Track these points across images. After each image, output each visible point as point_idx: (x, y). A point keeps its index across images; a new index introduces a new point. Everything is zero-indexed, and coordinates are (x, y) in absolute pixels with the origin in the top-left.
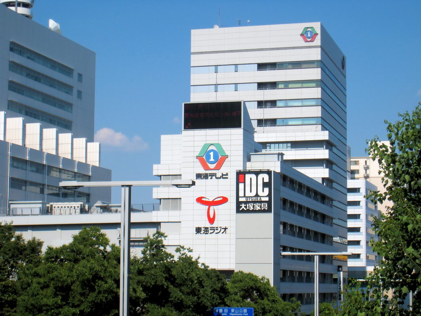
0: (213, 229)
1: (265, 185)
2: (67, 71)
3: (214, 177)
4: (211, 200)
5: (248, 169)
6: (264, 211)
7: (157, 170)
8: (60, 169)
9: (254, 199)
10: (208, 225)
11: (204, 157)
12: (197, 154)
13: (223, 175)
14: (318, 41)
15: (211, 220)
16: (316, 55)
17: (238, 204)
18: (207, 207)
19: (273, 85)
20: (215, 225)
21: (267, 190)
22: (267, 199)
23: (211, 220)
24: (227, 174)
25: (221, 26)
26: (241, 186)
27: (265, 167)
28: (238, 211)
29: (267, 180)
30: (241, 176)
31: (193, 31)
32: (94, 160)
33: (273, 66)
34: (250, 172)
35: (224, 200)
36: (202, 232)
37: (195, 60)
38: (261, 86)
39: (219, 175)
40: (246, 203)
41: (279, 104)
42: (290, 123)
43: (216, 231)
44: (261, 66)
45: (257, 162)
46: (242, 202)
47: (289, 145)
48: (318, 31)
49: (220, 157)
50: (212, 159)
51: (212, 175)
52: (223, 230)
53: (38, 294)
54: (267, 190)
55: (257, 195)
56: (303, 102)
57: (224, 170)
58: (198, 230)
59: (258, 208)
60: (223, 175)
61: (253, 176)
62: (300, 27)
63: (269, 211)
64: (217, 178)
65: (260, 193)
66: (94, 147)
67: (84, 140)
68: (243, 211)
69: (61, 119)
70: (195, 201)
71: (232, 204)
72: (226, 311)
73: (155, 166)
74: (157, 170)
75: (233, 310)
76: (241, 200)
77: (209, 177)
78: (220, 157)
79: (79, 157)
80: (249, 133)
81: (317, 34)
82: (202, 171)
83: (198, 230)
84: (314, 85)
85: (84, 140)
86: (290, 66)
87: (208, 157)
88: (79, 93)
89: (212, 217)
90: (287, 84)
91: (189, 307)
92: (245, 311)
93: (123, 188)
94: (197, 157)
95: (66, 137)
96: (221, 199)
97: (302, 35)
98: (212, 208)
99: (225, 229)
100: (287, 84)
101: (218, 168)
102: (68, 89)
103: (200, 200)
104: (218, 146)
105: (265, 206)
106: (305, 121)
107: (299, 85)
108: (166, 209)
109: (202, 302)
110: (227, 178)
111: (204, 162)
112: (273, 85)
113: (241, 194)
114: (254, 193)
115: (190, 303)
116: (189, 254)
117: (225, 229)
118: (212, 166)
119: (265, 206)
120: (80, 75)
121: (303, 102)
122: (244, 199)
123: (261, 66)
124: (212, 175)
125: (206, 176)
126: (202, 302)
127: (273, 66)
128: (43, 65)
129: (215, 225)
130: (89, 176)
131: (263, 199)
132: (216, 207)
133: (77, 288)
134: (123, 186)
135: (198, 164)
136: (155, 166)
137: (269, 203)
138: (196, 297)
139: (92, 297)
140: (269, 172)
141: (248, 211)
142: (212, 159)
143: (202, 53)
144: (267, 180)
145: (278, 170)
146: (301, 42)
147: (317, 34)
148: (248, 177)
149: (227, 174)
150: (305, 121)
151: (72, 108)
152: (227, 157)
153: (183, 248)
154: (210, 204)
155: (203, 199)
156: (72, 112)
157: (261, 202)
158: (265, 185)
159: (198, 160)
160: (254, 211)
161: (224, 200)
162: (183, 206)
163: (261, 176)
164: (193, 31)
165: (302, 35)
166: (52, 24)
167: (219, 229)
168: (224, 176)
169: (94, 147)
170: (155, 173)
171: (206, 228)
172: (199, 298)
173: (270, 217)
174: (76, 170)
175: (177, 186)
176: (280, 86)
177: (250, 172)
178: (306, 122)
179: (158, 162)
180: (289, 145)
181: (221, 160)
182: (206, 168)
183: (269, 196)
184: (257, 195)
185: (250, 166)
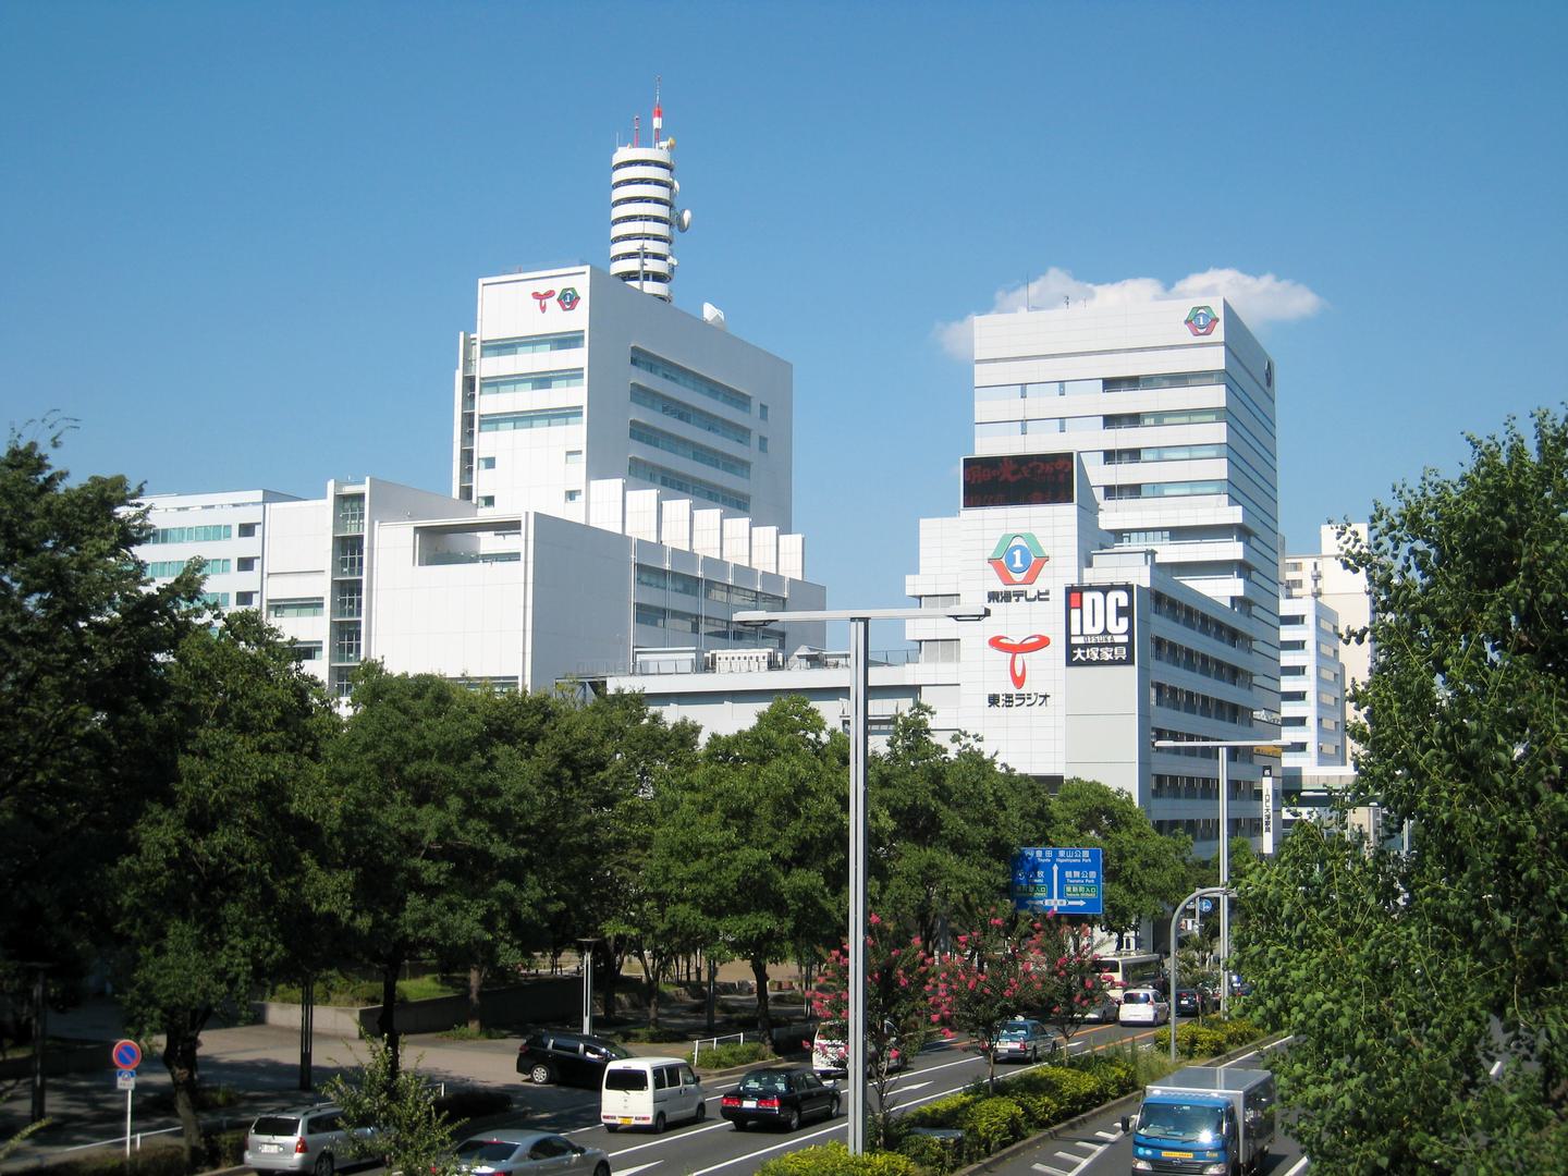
0: (1021, 697)
1: (1121, 612)
2: (740, 400)
4: (1017, 642)
5: (1087, 582)
6: (1120, 662)
7: (914, 585)
8: (728, 586)
9: (1101, 639)
10: (1013, 690)
11: (1003, 560)
12: (990, 554)
13: (1039, 594)
14: (1219, 333)
15: (1019, 681)
16: (1216, 359)
18: (1010, 655)
19: (1134, 419)
20: (1024, 690)
21: (1124, 622)
22: (1125, 639)
23: (1019, 681)
24: (1047, 593)
26: (1075, 614)
27: (1121, 580)
28: (1070, 662)
29: (1124, 602)
30: (1074, 594)
32: (792, 568)
33: (1133, 382)
34: (1091, 588)
35: (1043, 642)
36: (1001, 703)
38: (1111, 421)
39: (1031, 595)
40: (1085, 646)
41: (1145, 455)
42: (1167, 492)
43: (1028, 702)
44: (1110, 384)
45: (1105, 569)
46: (1076, 646)
47: (1167, 534)
48: (1220, 314)
49: (1033, 559)
50: (1018, 564)
51: (1019, 595)
52: (1040, 700)
53: (693, 823)
54: (1124, 622)
55: (1105, 632)
56: (1192, 450)
57: (1041, 584)
59: (1108, 657)
60: (1039, 594)
61: (1099, 596)
63: (1129, 661)
64: (1028, 600)
65: (1112, 628)
66: (792, 543)
67: (774, 529)
68: (1079, 663)
69: (728, 491)
70: (987, 645)
72: (1049, 853)
73: (909, 579)
74: (914, 585)
75: (1062, 853)
76: (1074, 641)
77: (1014, 599)
78: (1033, 559)
79: (764, 562)
80: (1088, 511)
81: (1217, 320)
82: (1000, 587)
83: (993, 700)
84: (1213, 418)
85: (774, 529)
86: (1166, 383)
88: (763, 440)
89: (1019, 673)
90: (1160, 417)
91: (979, 847)
92: (1086, 853)
95: (739, 525)
96: (1036, 640)
97: (1187, 322)
99: (1046, 697)
100: (1160, 417)
101: (1030, 580)
102: (741, 433)
103: (996, 642)
104: (1030, 538)
105: (1122, 653)
106: (1195, 487)
107: (1184, 419)
108: (930, 659)
109: (1002, 837)
110: (1047, 600)
112: (1134, 419)
113: (1075, 629)
114: (1099, 628)
115: (979, 839)
116: (976, 746)
117: (1046, 697)
118: (1018, 577)
119: (1122, 653)
120: (764, 408)
121: (1192, 450)
122: (1080, 640)
123: (1110, 384)
124: (1019, 595)
125: (1007, 597)
126: (1002, 837)
127: (1133, 382)
128: (695, 390)
130: (784, 599)
131: (1118, 639)
132: (1026, 656)
133: (764, 811)
134: (853, 619)
135: (991, 571)
136: (909, 579)
137: (1129, 646)
138: (991, 829)
139: (794, 828)
140: (1128, 588)
141: (1089, 663)
142: (1018, 564)
143: (995, 360)
144: (1124, 602)
145: (1146, 583)
147: (1217, 320)
148: (1087, 597)
149: (1047, 593)
150: (1195, 487)
151: (749, 471)
152: (1047, 559)
153: (965, 734)
154: (1014, 650)
155: (1002, 641)
156: (749, 478)
157: (1113, 645)
158: (1121, 612)
160: (1100, 663)
161: (1043, 642)
163: (1112, 596)
165: (1187, 322)
166: (710, 312)
167: (1034, 697)
168: (1042, 597)
169: (792, 543)
170: (909, 591)
171: (1009, 696)
172: (996, 829)
173: (1132, 672)
174: (759, 588)
175: (955, 617)
176: (1147, 421)
177: (1091, 588)
178: (1199, 490)
179: (916, 571)
180: (1167, 534)
181: (1036, 564)
182: (1008, 581)
183: (1130, 632)
184: (1105, 632)
185: (1090, 576)
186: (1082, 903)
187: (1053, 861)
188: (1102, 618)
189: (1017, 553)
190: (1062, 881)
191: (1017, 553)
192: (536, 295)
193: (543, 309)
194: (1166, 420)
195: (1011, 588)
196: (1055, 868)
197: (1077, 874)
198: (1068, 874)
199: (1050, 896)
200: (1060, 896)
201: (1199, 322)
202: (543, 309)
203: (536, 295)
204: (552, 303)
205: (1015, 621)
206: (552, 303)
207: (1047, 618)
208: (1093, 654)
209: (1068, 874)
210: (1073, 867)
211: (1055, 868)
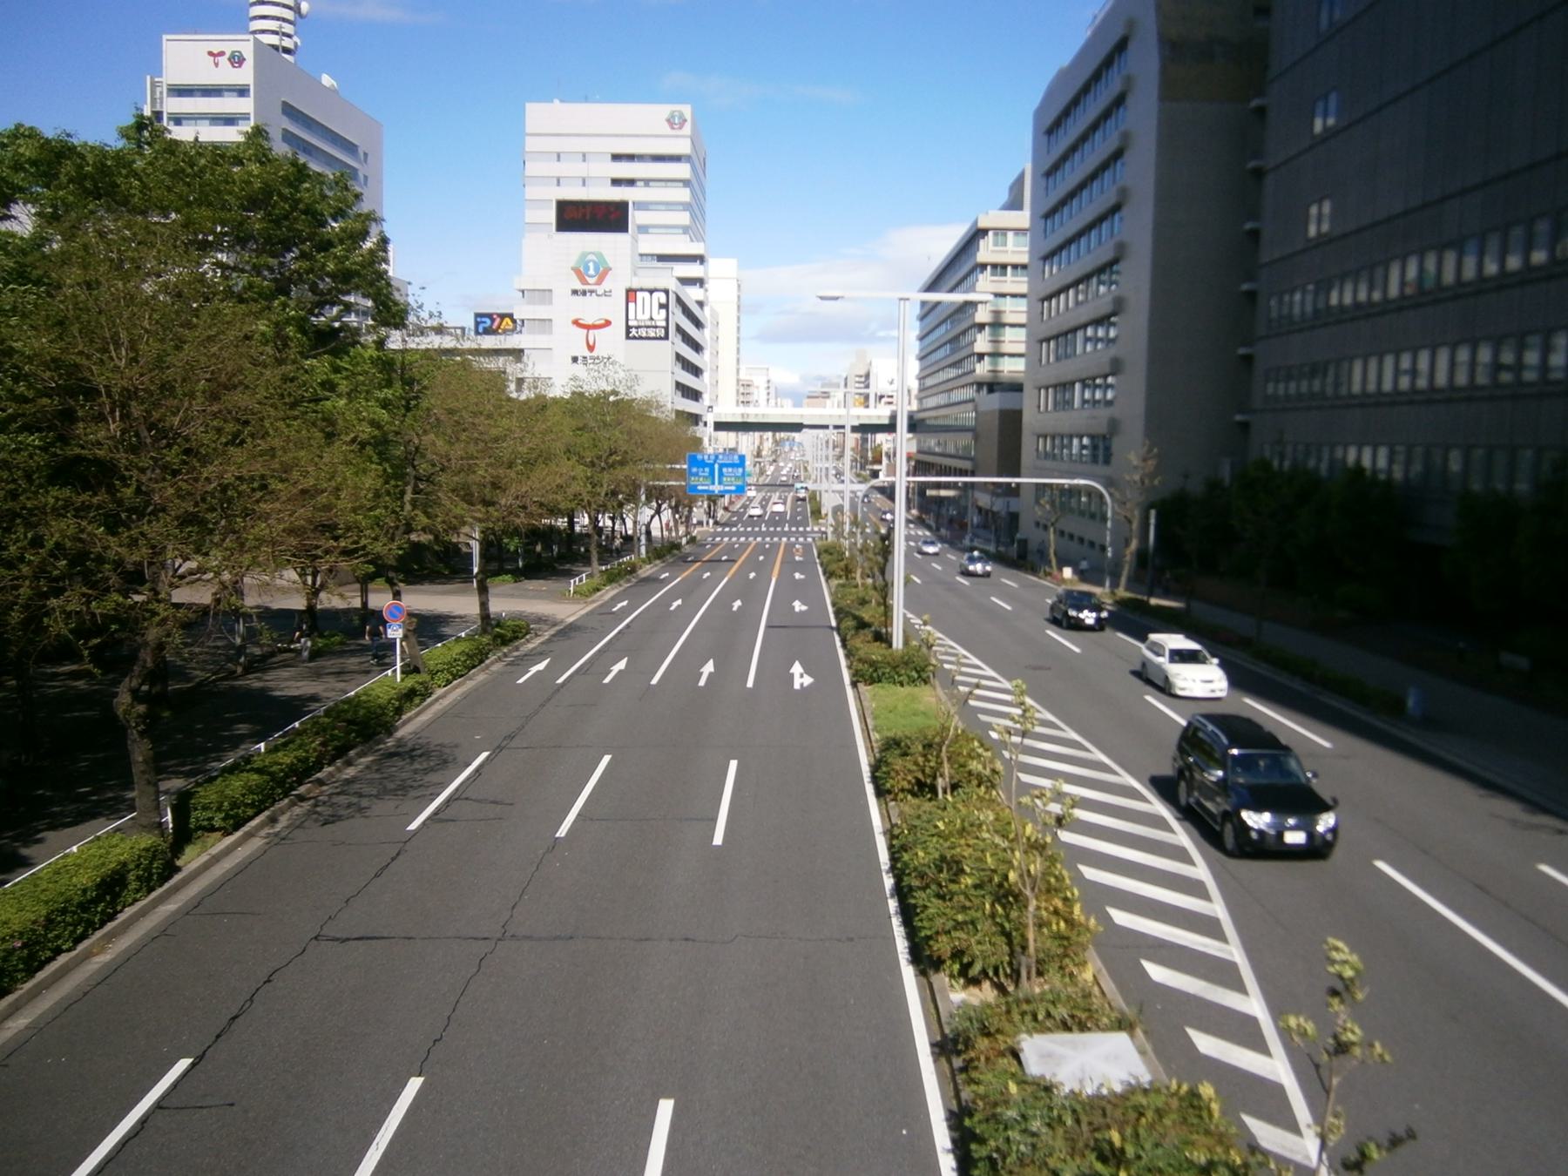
0: (594, 358)
1: (661, 306)
2: (350, 148)
3: (594, 294)
4: (590, 323)
5: (635, 286)
6: (661, 338)
9: (649, 323)
12: (572, 264)
14: (687, 129)
15: (591, 348)
17: (628, 328)
18: (585, 331)
20: (595, 354)
22: (664, 324)
23: (591, 348)
24: (610, 291)
25: (562, 101)
26: (631, 305)
28: (628, 337)
29: (663, 300)
30: (631, 294)
31: (529, 106)
33: (631, 158)
35: (608, 323)
36: (579, 362)
37: (531, 144)
38: (616, 182)
40: (637, 328)
44: (616, 157)
48: (688, 116)
50: (592, 272)
51: (591, 292)
54: (663, 312)
56: (669, 206)
57: (606, 285)
58: (575, 360)
59: (653, 335)
61: (647, 295)
62: (665, 110)
63: (666, 337)
64: (598, 295)
68: (634, 338)
71: (619, 328)
77: (588, 294)
81: (685, 121)
82: (579, 286)
83: (575, 360)
87: (587, 268)
89: (591, 343)
90: (647, 182)
93: (902, 302)
94: (572, 269)
98: (591, 331)
101: (599, 282)
103: (576, 323)
104: (600, 255)
105: (662, 333)
107: (663, 184)
111: (580, 275)
112: (631, 182)
113: (631, 316)
114: (647, 316)
118: (591, 280)
120: (366, 154)
121: (669, 206)
123: (616, 157)
124: (591, 292)
125: (584, 293)
127: (631, 158)
129: (595, 354)
131: (659, 324)
132: (596, 331)
134: (901, 299)
140: (667, 292)
141: (641, 338)
142: (592, 272)
144: (663, 300)
146: (667, 130)
147: (685, 121)
148: (640, 295)
149: (610, 291)
154: (588, 327)
157: (656, 327)
158: (661, 306)
159: (572, 272)
161: (608, 323)
162: (554, 329)
163: (656, 295)
164: (529, 106)
166: (327, 80)
168: (607, 294)
171: (585, 358)
176: (639, 183)
182: (584, 282)
183: (667, 320)
184: (652, 319)
186: (733, 488)
187: (715, 462)
188: (647, 310)
189: (591, 265)
190: (721, 474)
191: (591, 265)
192: (211, 54)
193: (217, 65)
194: (651, 184)
195: (587, 288)
196: (716, 466)
197: (730, 470)
198: (724, 470)
199: (713, 483)
200: (720, 483)
201: (674, 122)
202: (217, 65)
203: (211, 54)
204: (223, 60)
205: (590, 310)
206: (223, 60)
207: (613, 308)
208: (643, 332)
209: (724, 470)
210: (727, 466)
211: (716, 466)
